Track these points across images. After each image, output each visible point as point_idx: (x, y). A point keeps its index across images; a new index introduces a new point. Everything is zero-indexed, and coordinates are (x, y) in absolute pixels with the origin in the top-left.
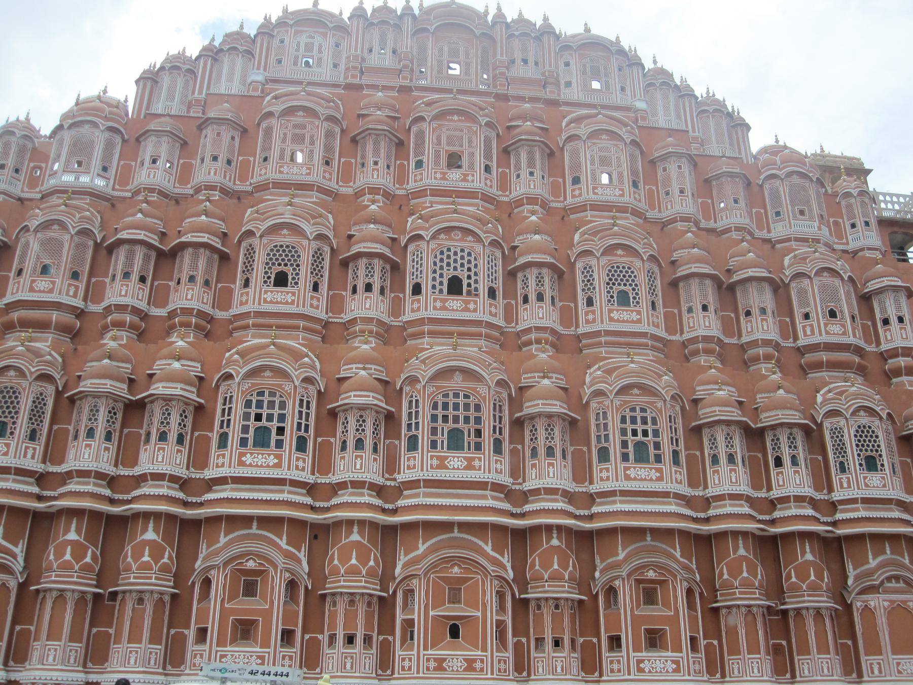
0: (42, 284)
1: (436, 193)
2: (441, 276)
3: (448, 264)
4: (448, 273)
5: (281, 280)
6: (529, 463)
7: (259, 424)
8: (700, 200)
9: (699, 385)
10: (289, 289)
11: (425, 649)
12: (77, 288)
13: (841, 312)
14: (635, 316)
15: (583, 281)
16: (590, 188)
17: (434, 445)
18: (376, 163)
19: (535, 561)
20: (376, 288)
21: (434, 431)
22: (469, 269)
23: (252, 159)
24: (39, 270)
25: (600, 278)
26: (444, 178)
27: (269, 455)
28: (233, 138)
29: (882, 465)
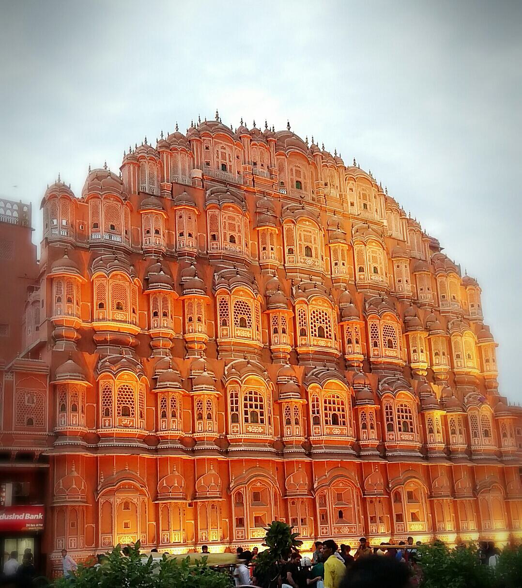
1: (302, 271)
2: (315, 326)
3: (317, 320)
4: (318, 325)
5: (243, 324)
6: (361, 431)
7: (252, 410)
9: (422, 392)
10: (247, 329)
11: (333, 524)
13: (473, 355)
15: (372, 332)
16: (369, 274)
19: (369, 481)
22: (326, 322)
27: (259, 427)
29: (490, 434)
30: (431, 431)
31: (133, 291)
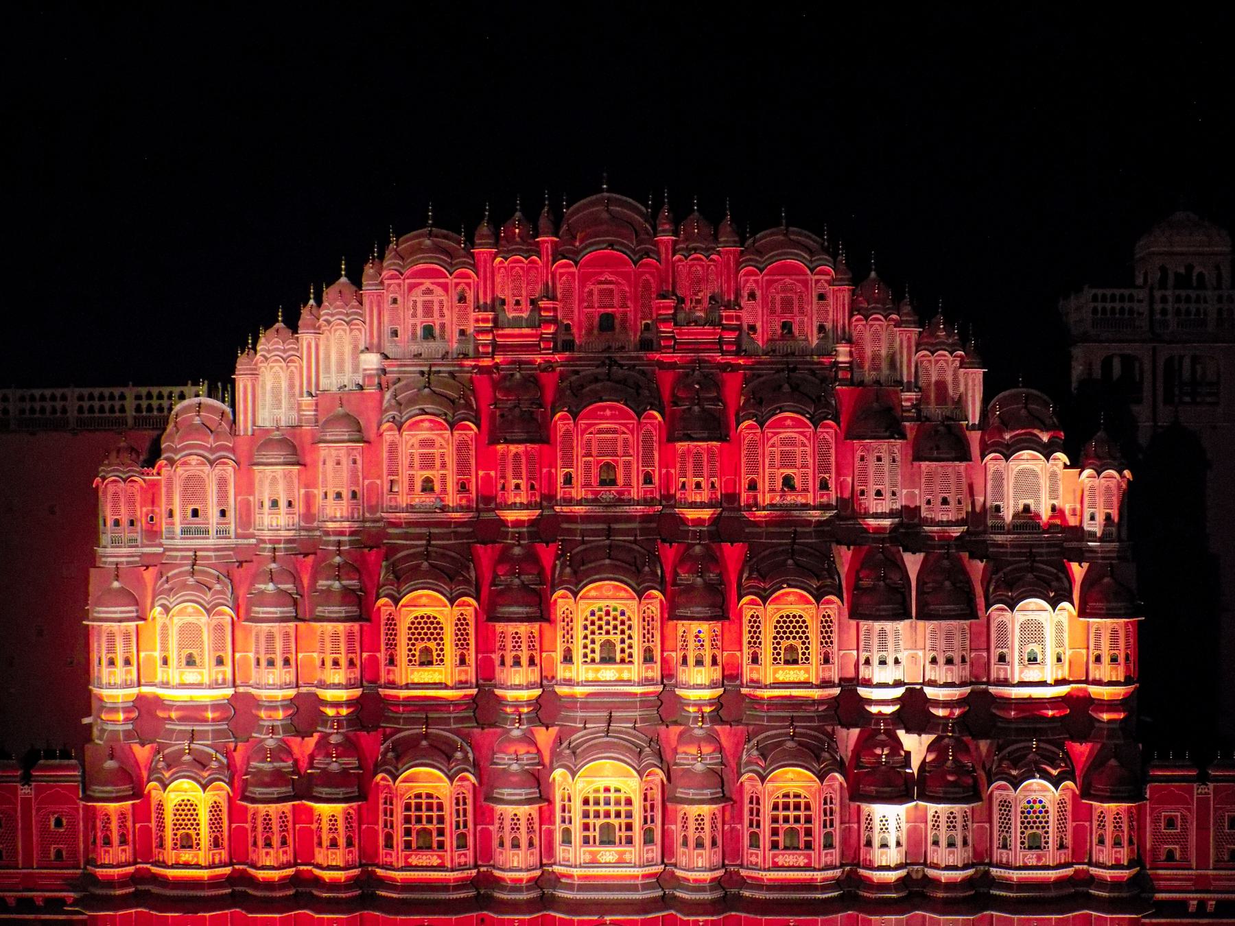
0: (191, 676)
4: (600, 638)
8: (905, 491)
12: (224, 673)
14: (802, 676)
16: (768, 496)
17: (586, 841)
18: (517, 487)
20: (524, 661)
21: (586, 827)
22: (623, 632)
23: (378, 482)
24: (184, 662)
25: (768, 633)
26: (595, 501)
28: (355, 462)
29: (1047, 843)
30: (869, 843)
31: (219, 628)
